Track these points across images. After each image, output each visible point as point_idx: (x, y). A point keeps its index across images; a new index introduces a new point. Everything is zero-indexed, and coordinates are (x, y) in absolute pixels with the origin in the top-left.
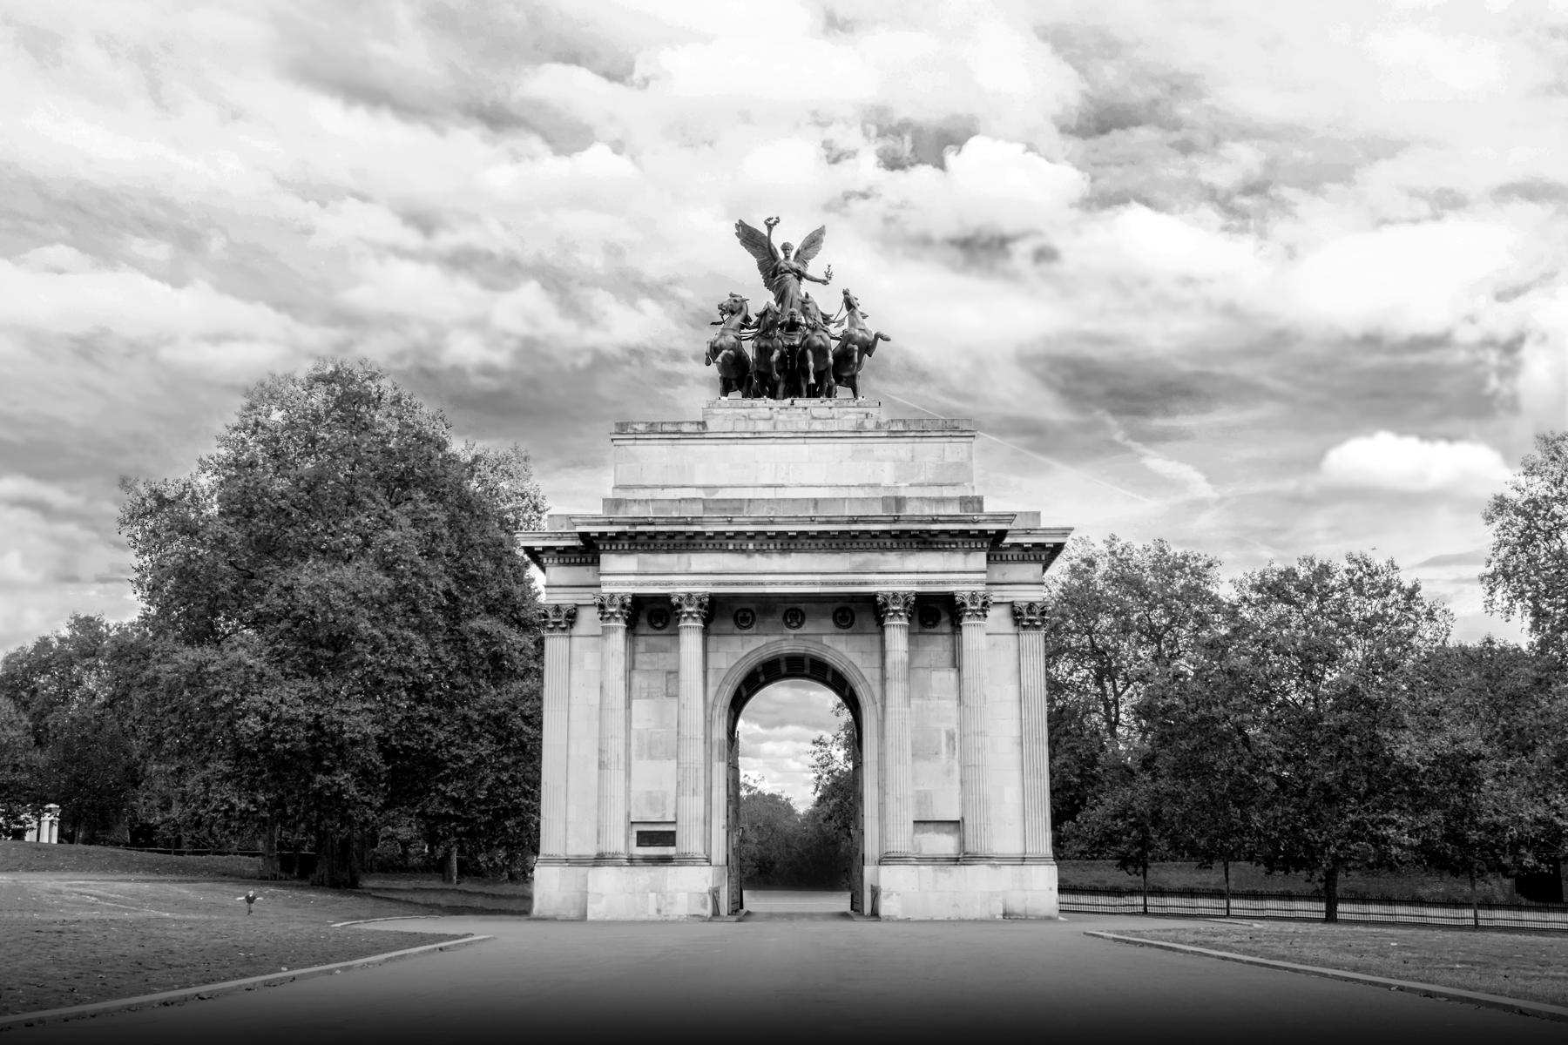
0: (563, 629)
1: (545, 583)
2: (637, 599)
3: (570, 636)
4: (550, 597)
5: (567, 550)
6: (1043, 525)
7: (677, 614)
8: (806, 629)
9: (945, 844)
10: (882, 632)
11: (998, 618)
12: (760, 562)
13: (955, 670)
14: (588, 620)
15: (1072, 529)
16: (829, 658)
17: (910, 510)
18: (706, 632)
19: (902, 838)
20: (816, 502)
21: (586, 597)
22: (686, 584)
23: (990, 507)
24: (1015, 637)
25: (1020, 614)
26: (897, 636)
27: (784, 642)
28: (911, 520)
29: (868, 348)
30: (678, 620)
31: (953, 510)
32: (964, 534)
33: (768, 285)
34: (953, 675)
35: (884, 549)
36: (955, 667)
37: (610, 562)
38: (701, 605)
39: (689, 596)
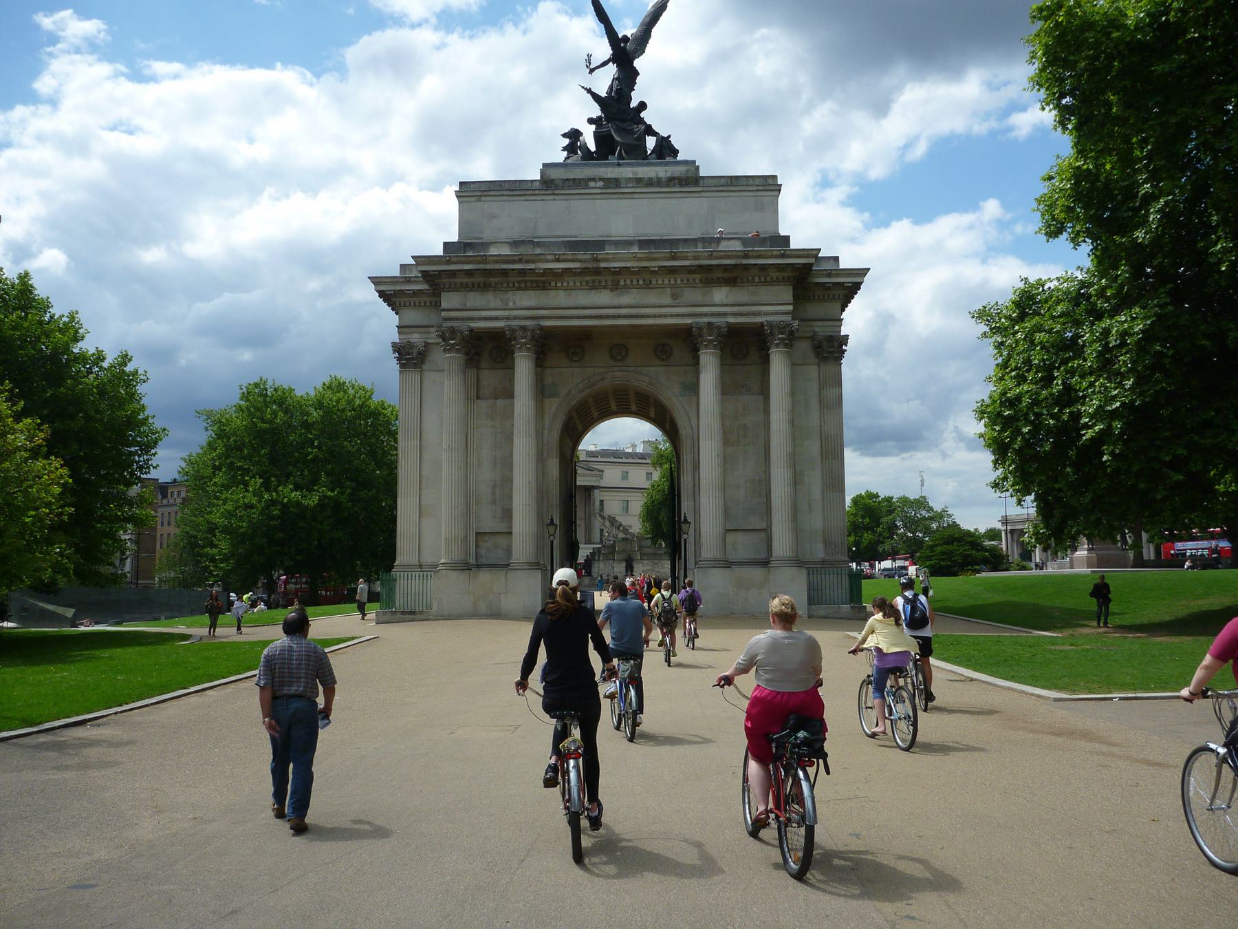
1: (398, 325)
3: (421, 371)
4: (403, 337)
5: (416, 293)
6: (841, 267)
7: (513, 346)
10: (696, 362)
11: (804, 346)
13: (761, 397)
15: (869, 269)
18: (540, 363)
22: (519, 318)
23: (794, 245)
24: (816, 367)
25: (819, 347)
27: (612, 375)
36: (762, 394)
37: (449, 300)
38: (533, 338)
39: (524, 328)
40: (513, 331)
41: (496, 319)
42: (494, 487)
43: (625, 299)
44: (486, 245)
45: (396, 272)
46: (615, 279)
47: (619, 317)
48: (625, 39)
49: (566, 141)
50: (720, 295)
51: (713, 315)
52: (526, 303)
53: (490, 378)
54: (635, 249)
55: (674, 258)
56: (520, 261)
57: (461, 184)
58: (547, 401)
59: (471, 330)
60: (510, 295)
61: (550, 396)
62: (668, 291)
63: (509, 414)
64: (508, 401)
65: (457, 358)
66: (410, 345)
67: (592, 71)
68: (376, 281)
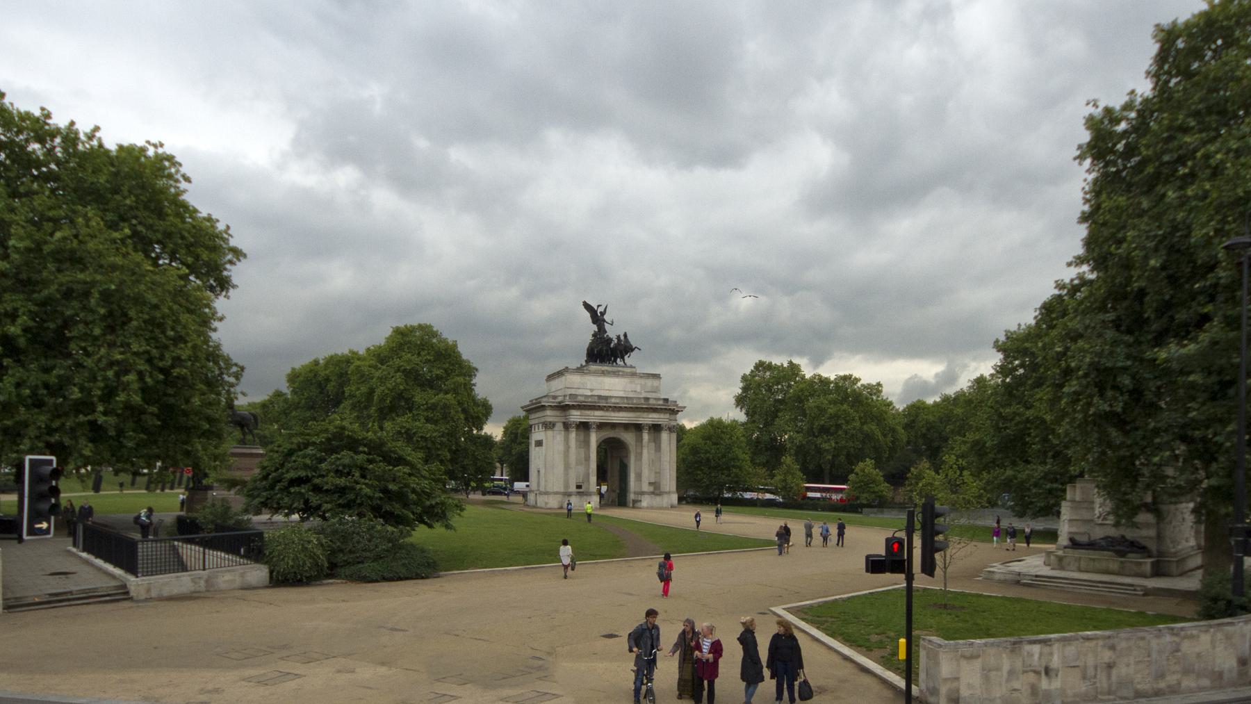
2: (582, 423)
8: (617, 430)
9: (651, 489)
12: (613, 414)
16: (622, 439)
17: (651, 402)
19: (646, 488)
20: (627, 398)
26: (646, 436)
28: (654, 405)
29: (632, 350)
31: (661, 402)
32: (666, 409)
33: (594, 323)
34: (653, 444)
35: (644, 412)
59: (580, 422)
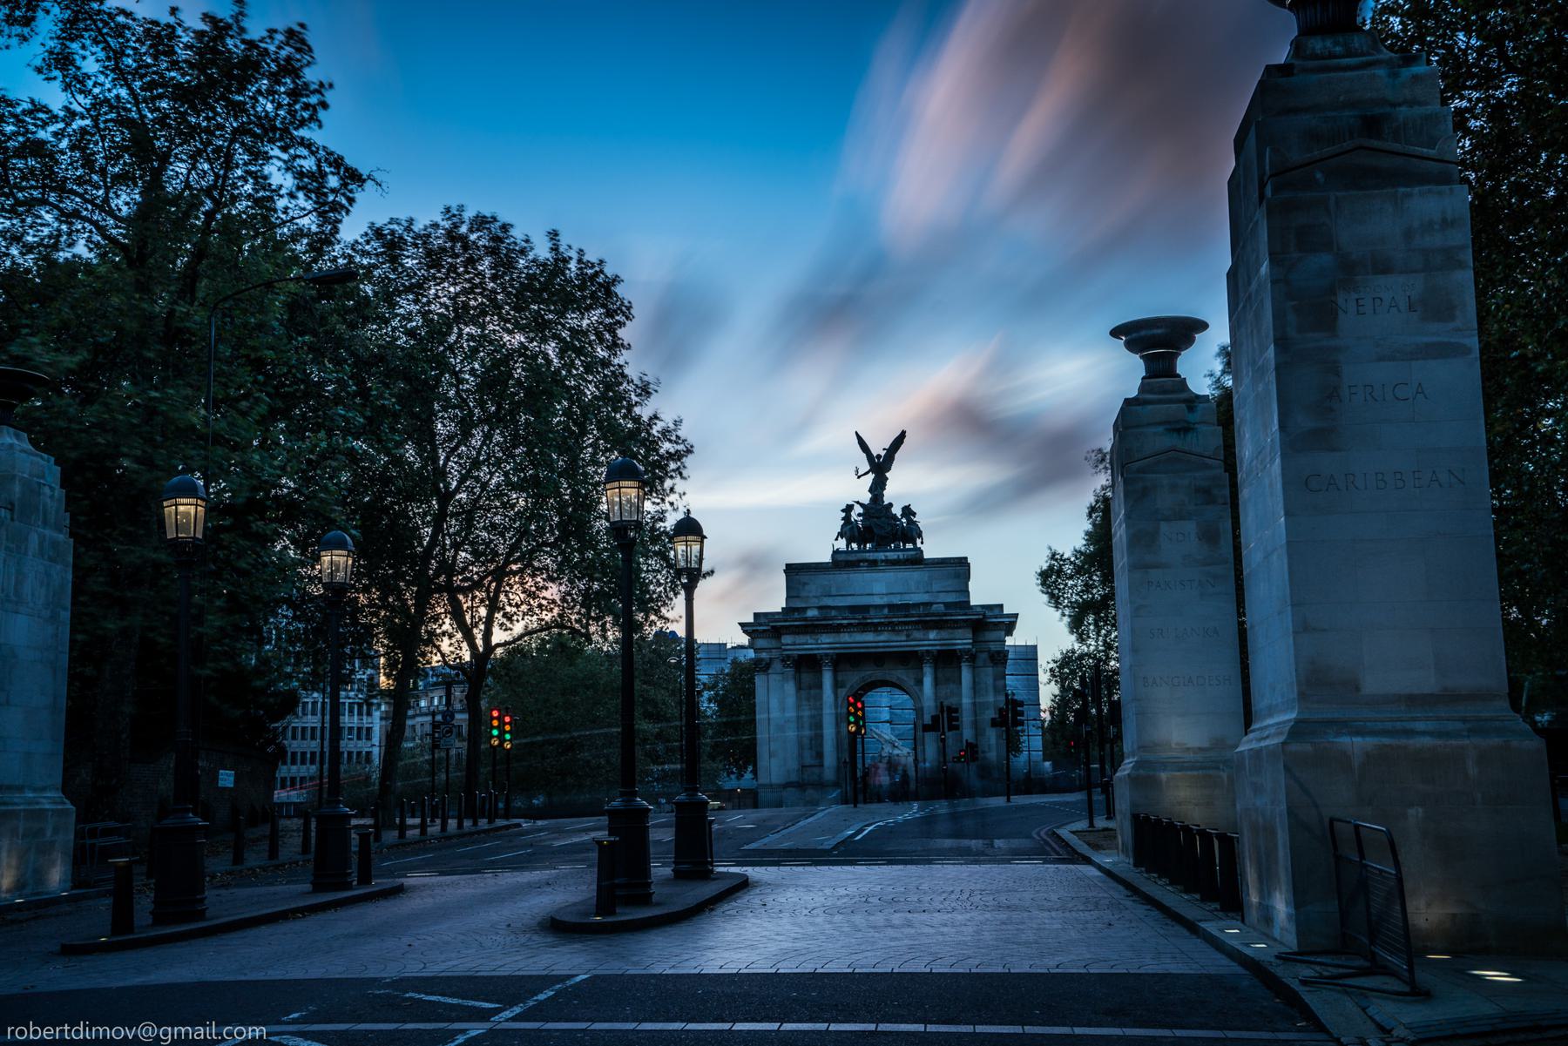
0: (765, 671)
5: (764, 631)
10: (922, 668)
14: (777, 666)
18: (835, 672)
21: (775, 654)
30: (821, 667)
37: (787, 639)
40: (821, 655)
41: (812, 649)
42: (811, 740)
43: (883, 637)
44: (804, 609)
45: (751, 620)
46: (875, 628)
47: (879, 647)
48: (879, 456)
49: (843, 515)
50: (932, 635)
51: (929, 645)
52: (828, 641)
53: (807, 678)
54: (886, 611)
55: (906, 616)
56: (824, 620)
57: (787, 565)
58: (839, 690)
60: (819, 636)
61: (841, 687)
62: (905, 633)
63: (819, 697)
64: (818, 691)
65: (790, 671)
66: (762, 660)
67: (859, 477)
68: (740, 624)
